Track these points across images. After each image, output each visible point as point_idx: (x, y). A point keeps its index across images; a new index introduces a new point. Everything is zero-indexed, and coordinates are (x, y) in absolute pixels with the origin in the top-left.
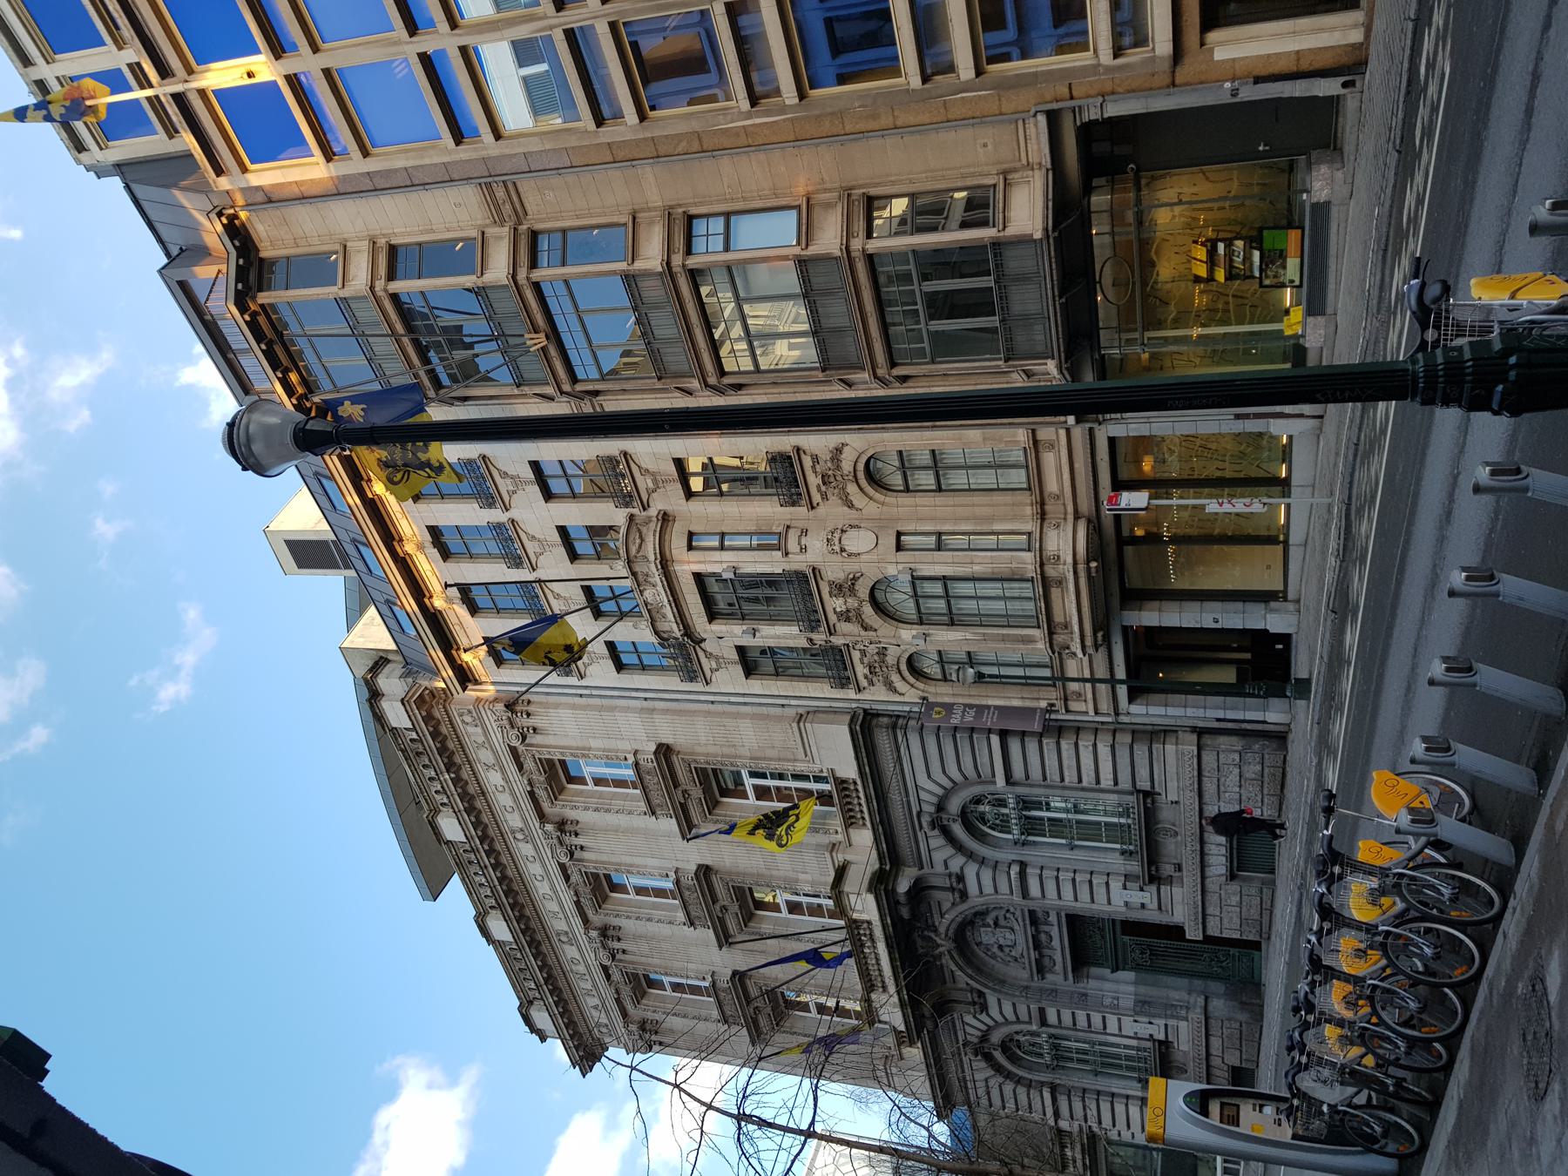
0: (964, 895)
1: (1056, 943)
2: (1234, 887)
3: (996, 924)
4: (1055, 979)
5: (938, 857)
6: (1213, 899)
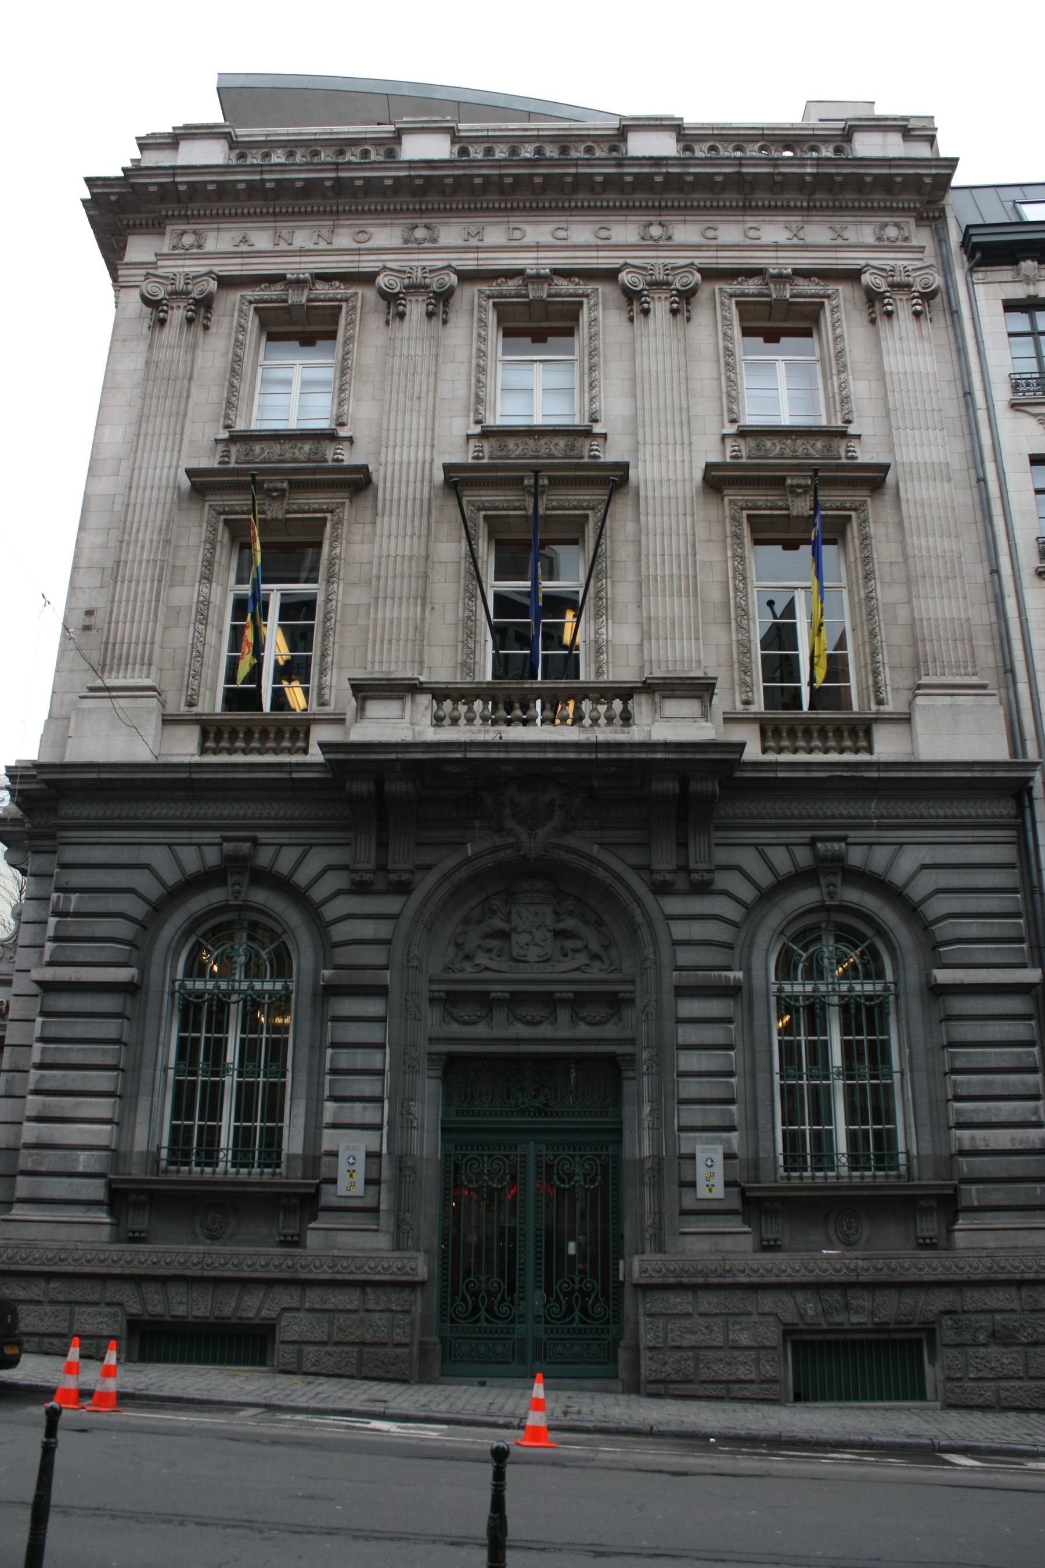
0: (662, 889)
1: (521, 1030)
2: (773, 1335)
3: (560, 934)
4: (432, 1020)
5: (748, 858)
6: (737, 1302)
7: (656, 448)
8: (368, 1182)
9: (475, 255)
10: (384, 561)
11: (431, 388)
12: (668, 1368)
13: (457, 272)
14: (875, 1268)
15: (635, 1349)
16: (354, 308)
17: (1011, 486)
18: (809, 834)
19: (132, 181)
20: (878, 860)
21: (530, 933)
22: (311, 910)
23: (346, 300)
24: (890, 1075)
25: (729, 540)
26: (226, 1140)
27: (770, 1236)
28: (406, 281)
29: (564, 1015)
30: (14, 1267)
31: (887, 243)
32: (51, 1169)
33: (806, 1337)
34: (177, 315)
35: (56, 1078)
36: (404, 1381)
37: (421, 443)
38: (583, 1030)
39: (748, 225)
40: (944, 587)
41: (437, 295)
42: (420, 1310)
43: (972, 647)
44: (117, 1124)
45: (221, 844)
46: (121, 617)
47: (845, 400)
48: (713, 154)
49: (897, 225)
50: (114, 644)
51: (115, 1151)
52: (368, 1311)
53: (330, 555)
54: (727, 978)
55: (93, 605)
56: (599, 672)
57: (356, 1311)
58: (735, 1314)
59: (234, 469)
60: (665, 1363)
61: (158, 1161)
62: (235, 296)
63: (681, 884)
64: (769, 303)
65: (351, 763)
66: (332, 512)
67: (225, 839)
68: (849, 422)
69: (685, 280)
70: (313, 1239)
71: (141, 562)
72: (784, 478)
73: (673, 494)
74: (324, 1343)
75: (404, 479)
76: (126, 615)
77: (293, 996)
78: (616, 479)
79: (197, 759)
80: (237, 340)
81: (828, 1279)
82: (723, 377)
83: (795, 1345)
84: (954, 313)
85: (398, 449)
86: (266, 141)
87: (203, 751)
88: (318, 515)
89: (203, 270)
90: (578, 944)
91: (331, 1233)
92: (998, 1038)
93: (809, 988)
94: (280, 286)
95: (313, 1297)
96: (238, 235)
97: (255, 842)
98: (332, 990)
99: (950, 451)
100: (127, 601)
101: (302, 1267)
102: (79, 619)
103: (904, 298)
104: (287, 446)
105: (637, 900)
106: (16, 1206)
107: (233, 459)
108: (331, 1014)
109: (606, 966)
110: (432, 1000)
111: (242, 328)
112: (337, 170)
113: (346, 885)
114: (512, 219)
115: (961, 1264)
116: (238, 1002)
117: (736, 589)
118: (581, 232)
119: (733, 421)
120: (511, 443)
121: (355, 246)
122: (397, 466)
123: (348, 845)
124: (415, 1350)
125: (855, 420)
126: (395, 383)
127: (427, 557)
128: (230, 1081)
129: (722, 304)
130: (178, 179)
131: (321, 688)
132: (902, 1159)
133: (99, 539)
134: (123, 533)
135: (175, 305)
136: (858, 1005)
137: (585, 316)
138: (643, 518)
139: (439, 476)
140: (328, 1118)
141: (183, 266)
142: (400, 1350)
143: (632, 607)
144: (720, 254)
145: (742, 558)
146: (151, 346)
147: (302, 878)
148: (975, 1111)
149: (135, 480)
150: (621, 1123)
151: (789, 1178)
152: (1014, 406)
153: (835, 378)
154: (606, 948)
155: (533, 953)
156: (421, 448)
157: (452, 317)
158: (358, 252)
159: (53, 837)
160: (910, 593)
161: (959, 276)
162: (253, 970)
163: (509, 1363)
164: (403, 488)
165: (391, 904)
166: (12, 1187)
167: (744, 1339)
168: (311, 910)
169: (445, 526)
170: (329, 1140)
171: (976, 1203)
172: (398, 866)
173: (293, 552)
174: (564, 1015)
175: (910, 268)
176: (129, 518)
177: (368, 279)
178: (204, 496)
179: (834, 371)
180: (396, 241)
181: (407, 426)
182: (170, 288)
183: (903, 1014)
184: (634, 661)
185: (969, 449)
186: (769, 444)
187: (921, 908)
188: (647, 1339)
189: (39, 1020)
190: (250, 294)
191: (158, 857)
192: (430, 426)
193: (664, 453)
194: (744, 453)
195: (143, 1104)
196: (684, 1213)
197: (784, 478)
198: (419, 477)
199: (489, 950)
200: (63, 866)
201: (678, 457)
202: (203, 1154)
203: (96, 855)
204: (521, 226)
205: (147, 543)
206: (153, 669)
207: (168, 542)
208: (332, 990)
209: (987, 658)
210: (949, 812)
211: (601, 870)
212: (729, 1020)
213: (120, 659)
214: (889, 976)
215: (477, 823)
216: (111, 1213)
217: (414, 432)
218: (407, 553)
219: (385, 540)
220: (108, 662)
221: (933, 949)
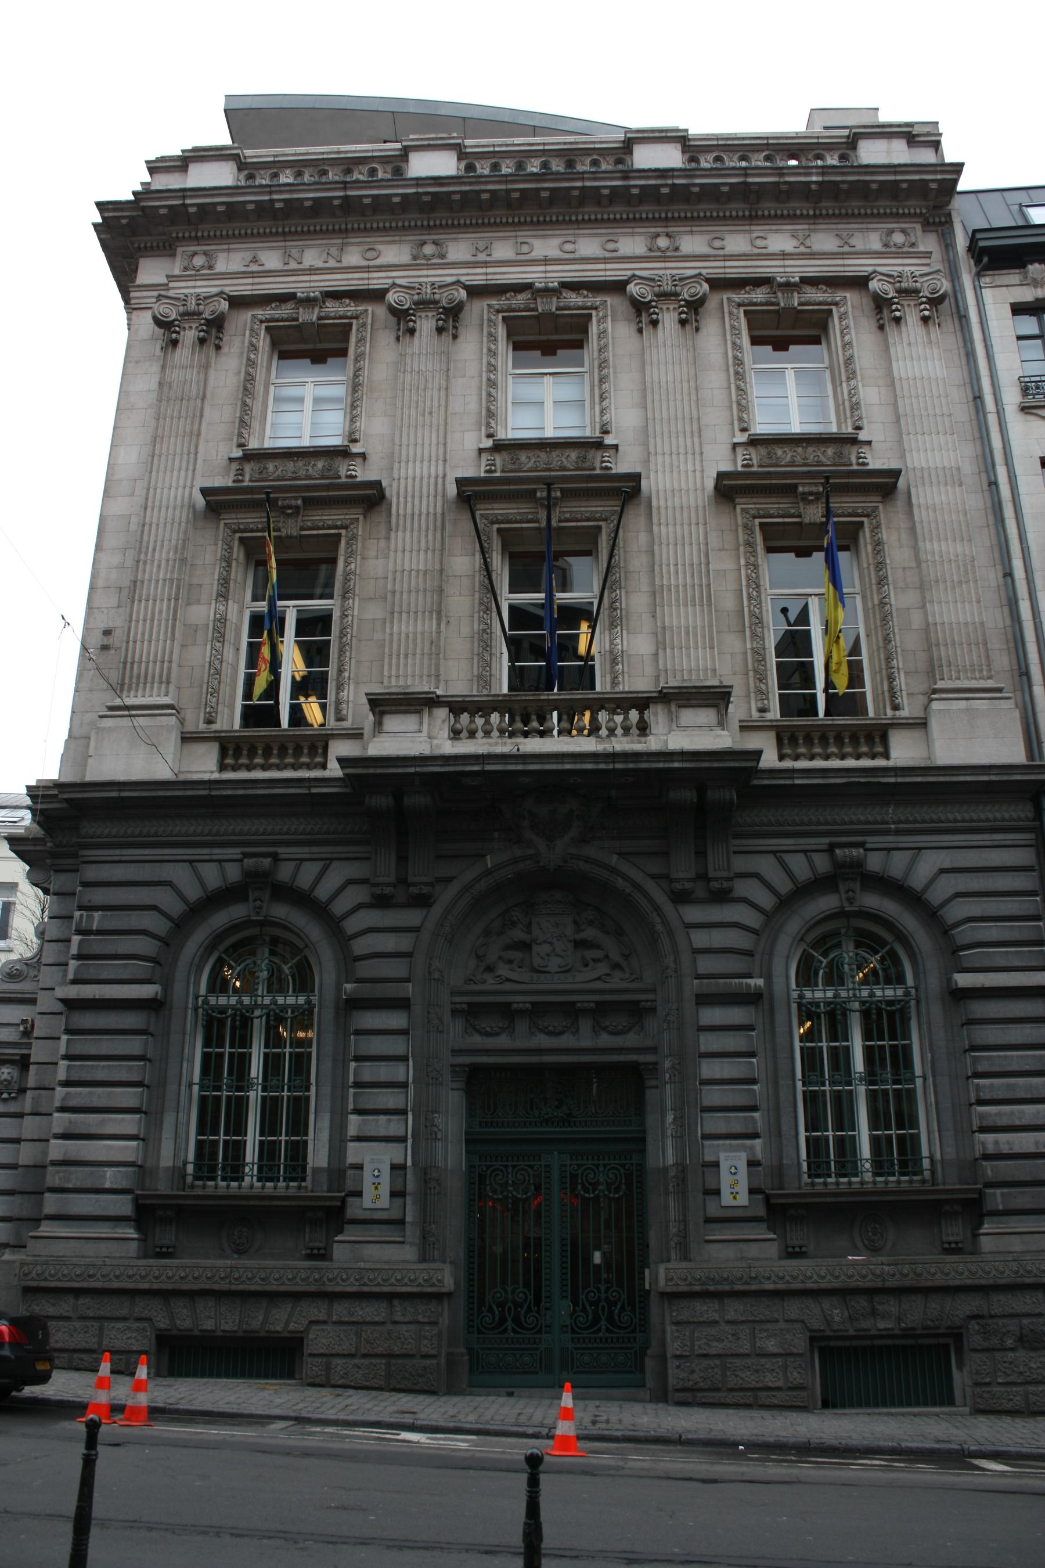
0: (681, 898)
1: (544, 1041)
2: (800, 1343)
4: (455, 1033)
5: (766, 866)
7: (667, 457)
8: (393, 1194)
9: (483, 270)
10: (398, 575)
11: (443, 403)
12: (695, 1377)
13: (466, 287)
14: (901, 1273)
15: (663, 1358)
16: (364, 325)
17: (1022, 489)
18: (827, 840)
19: (142, 204)
20: (897, 865)
21: (551, 944)
22: (333, 925)
23: (357, 318)
24: (912, 1080)
25: (742, 549)
26: (251, 1154)
27: (796, 1243)
28: (416, 297)
29: (585, 1025)
30: (43, 1284)
31: (893, 249)
32: (78, 1185)
33: (832, 1344)
34: (189, 335)
35: (82, 1095)
36: (432, 1393)
37: (434, 458)
38: (605, 1040)
39: (755, 235)
40: (957, 591)
41: (447, 311)
42: (447, 1322)
43: (987, 650)
44: (143, 1140)
45: (241, 860)
46: (139, 637)
47: (855, 407)
48: (718, 165)
49: (903, 231)
50: (133, 663)
51: (141, 1166)
52: (395, 1322)
53: (345, 571)
54: (748, 986)
55: (111, 625)
56: (614, 682)
57: (384, 1323)
58: (761, 1321)
59: (248, 487)
60: (693, 1372)
61: (184, 1176)
62: (246, 316)
63: (700, 892)
64: (777, 312)
65: (371, 777)
66: (346, 528)
67: (246, 855)
68: (859, 428)
69: (693, 290)
70: (339, 1252)
71: (157, 581)
72: (796, 486)
73: (685, 504)
74: (352, 1356)
75: (417, 494)
76: (143, 634)
77: (316, 1010)
78: (628, 490)
79: (216, 776)
80: (249, 359)
81: (854, 1285)
82: (733, 386)
83: (822, 1350)
84: (962, 318)
85: (410, 464)
86: (274, 162)
87: (222, 767)
88: (333, 531)
89: (215, 290)
90: (598, 954)
91: (357, 1246)
92: (1020, 1042)
93: (830, 994)
94: (290, 305)
95: (340, 1310)
96: (248, 256)
97: (276, 858)
98: (354, 1004)
99: (959, 454)
100: (145, 620)
101: (329, 1280)
102: (97, 639)
103: (912, 303)
104: (300, 464)
105: (657, 909)
106: (44, 1223)
107: (247, 477)
108: (353, 1027)
109: (627, 975)
110: (455, 1013)
111: (253, 348)
112: (345, 189)
113: (367, 899)
114: (519, 233)
115: (987, 1269)
116: (261, 1017)
117: (750, 598)
118: (589, 245)
119: (744, 430)
120: (523, 457)
121: (366, 263)
122: (410, 481)
123: (369, 859)
124: (443, 1361)
125: (865, 427)
126: (407, 398)
127: (441, 571)
128: (254, 1097)
129: (731, 313)
130: (188, 202)
131: (338, 703)
132: (926, 1163)
133: (116, 560)
134: (140, 552)
135: (186, 326)
136: (879, 1011)
137: (594, 329)
138: (655, 528)
139: (452, 490)
140: (352, 1131)
141: (195, 287)
142: (428, 1362)
143: (646, 617)
144: (728, 264)
145: (756, 566)
146: (163, 367)
147: (322, 893)
148: (999, 1114)
149: (150, 500)
150: (644, 1132)
151: (813, 1184)
152: (1024, 409)
153: (844, 384)
154: (626, 957)
155: (554, 964)
156: (433, 463)
157: (462, 331)
158: (368, 269)
159: (75, 856)
160: (923, 598)
161: (967, 281)
162: (276, 985)
163: (536, 1373)
164: (417, 502)
165: (412, 917)
166: (40, 1204)
167: (771, 1345)
168: (333, 925)
169: (459, 540)
170: (354, 1152)
171: (1001, 1207)
172: (417, 879)
173: (308, 568)
174: (585, 1025)
175: (917, 273)
176: (145, 538)
177: (377, 295)
178: (220, 514)
179: (844, 378)
180: (405, 258)
181: (419, 441)
182: (181, 309)
183: (924, 1019)
184: (649, 670)
185: (979, 452)
186: (779, 452)
187: (941, 913)
188: (674, 1347)
189: (64, 1037)
190: (261, 313)
191: (180, 874)
192: (441, 441)
193: (675, 463)
194: (755, 462)
195: (169, 1120)
196: (709, 1220)
197: (796, 486)
198: (432, 492)
199: (510, 962)
200: (85, 884)
201: (690, 467)
202: (229, 1169)
203: (118, 873)
204: (529, 240)
205: (163, 563)
206: (172, 687)
207: (183, 561)
208: (354, 1004)
209: (1002, 661)
210: (967, 816)
211: (620, 880)
212: (751, 1028)
213: (138, 678)
214: (910, 981)
215: (496, 835)
216: (139, 1229)
217: (426, 446)
218: (422, 567)
219: (399, 554)
220: (127, 681)
221: (953, 954)
